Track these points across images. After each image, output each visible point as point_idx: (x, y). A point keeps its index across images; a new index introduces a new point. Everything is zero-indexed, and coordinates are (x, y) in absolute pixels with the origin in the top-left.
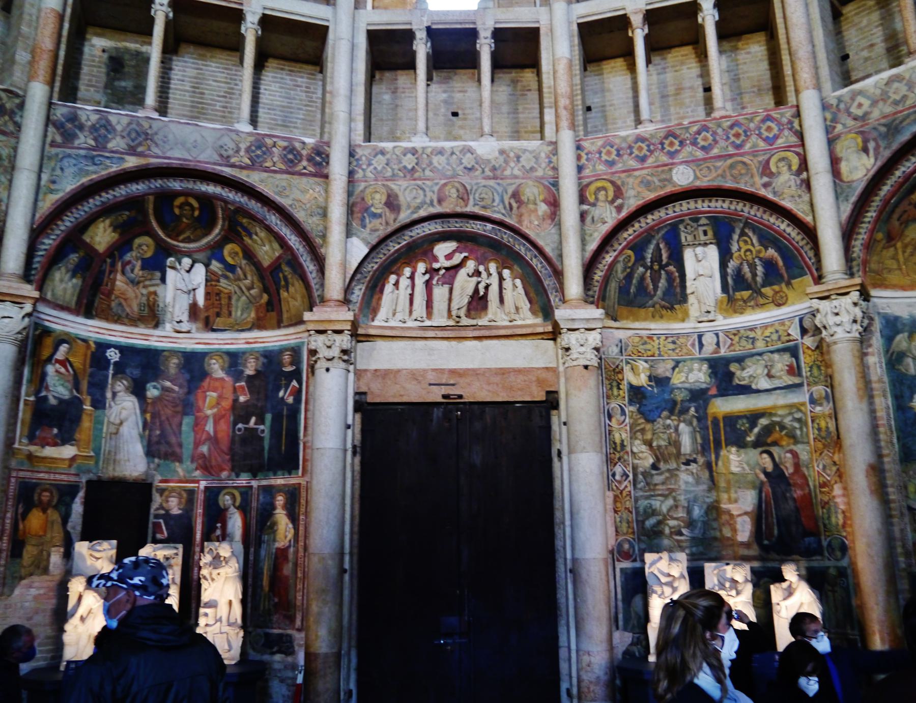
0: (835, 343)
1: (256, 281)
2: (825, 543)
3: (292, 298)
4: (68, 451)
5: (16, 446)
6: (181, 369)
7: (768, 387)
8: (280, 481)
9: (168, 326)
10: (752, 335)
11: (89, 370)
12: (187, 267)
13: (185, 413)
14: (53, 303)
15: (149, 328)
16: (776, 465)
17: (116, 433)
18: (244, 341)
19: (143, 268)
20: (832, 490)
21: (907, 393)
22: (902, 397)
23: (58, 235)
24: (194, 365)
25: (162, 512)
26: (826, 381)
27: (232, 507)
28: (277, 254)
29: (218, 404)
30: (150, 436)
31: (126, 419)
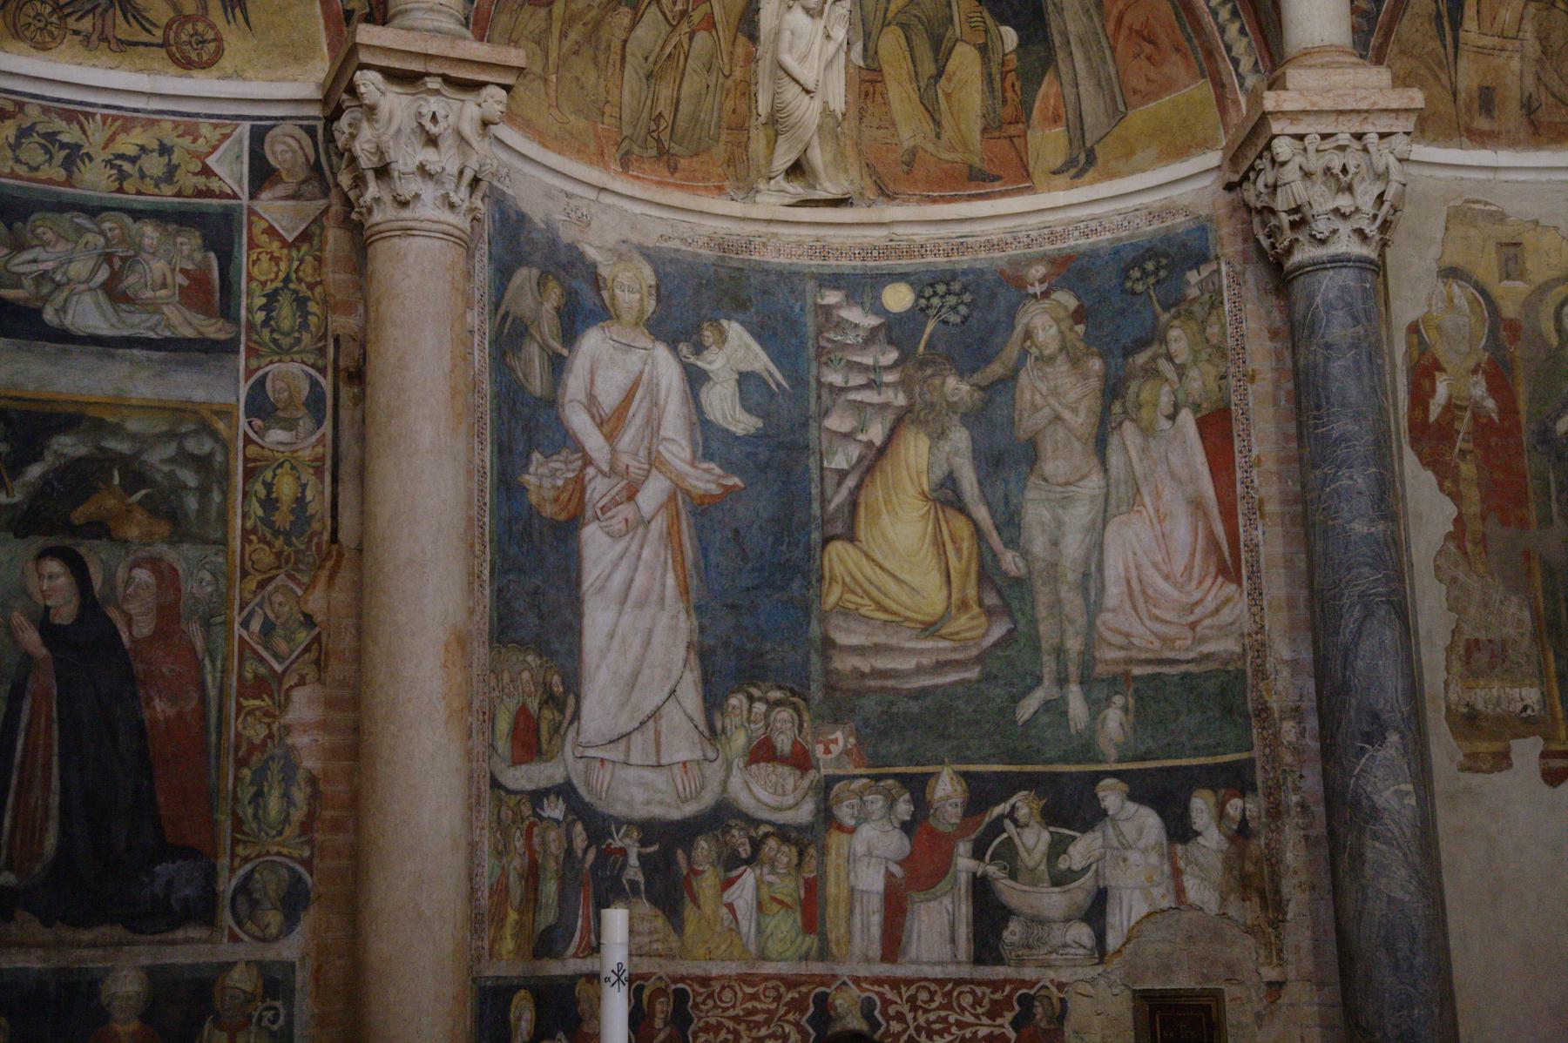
0: (407, 231)
2: (227, 885)
7: (104, 329)
10: (70, 135)
16: (90, 604)
20: (283, 707)
21: (520, 447)
22: (511, 452)
26: (322, 352)
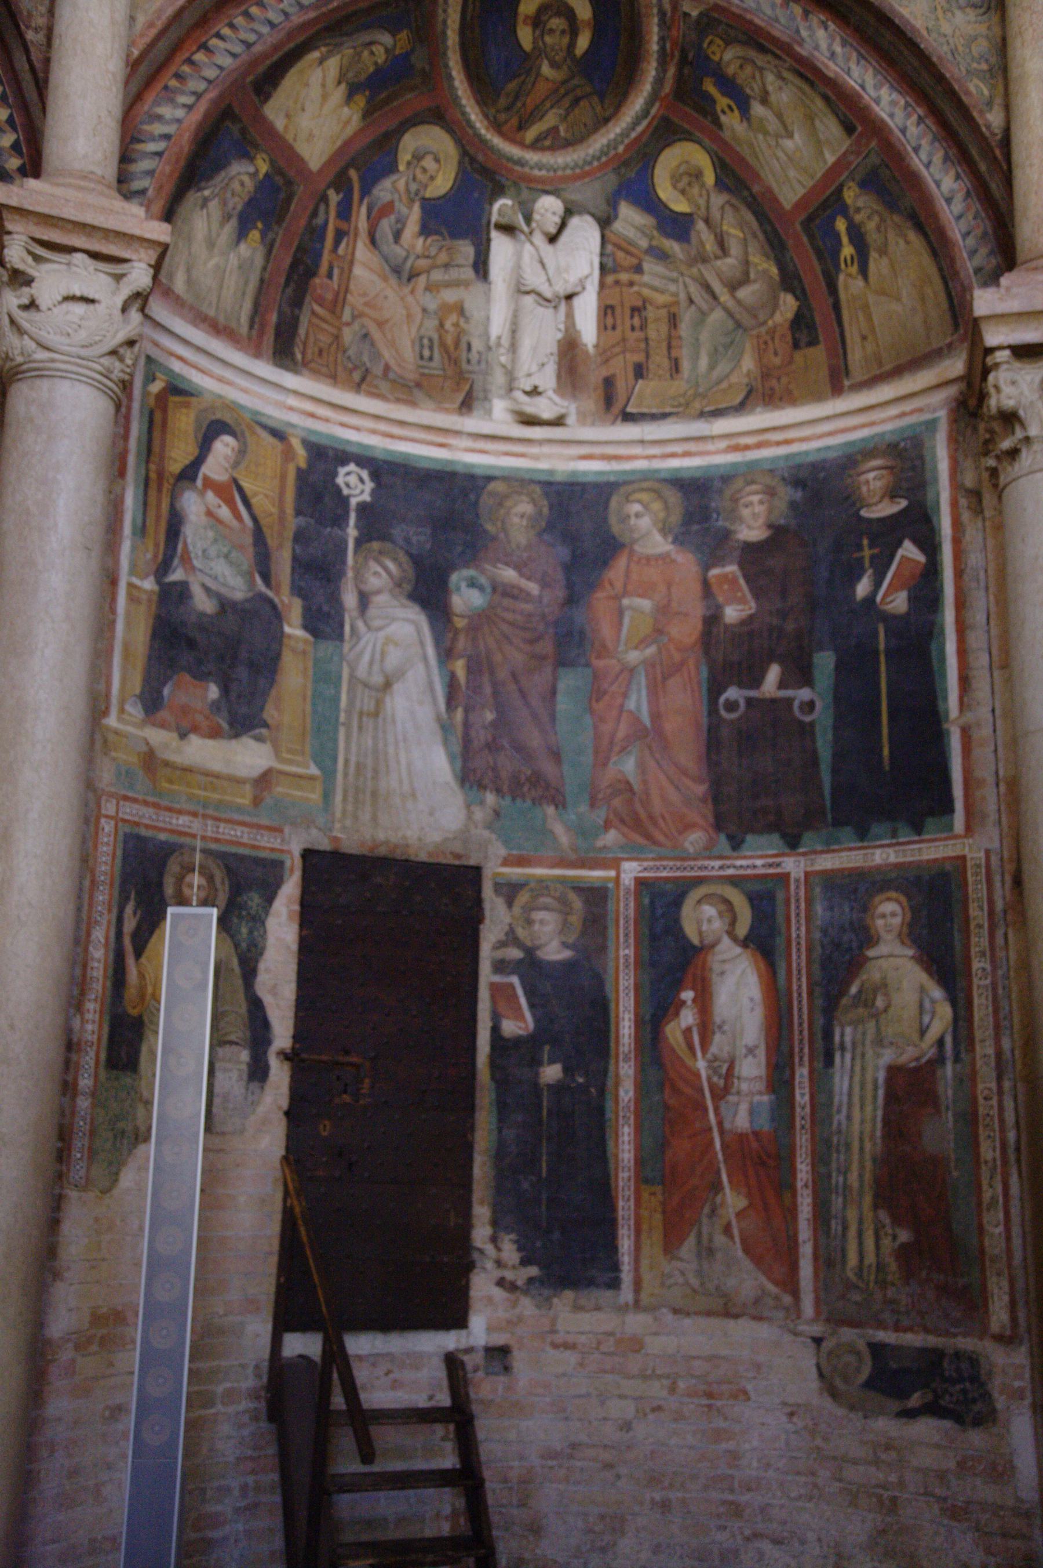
1: (756, 259)
3: (882, 292)
4: (248, 757)
5: (112, 721)
6: (539, 535)
8: (882, 855)
9: (500, 407)
11: (293, 523)
12: (551, 224)
13: (562, 662)
14: (192, 308)
15: (447, 411)
17: (376, 714)
18: (723, 444)
19: (425, 230)
23: (198, 96)
24: (580, 518)
25: (515, 953)
27: (726, 941)
28: (831, 159)
29: (659, 631)
30: (467, 725)
31: (400, 673)
